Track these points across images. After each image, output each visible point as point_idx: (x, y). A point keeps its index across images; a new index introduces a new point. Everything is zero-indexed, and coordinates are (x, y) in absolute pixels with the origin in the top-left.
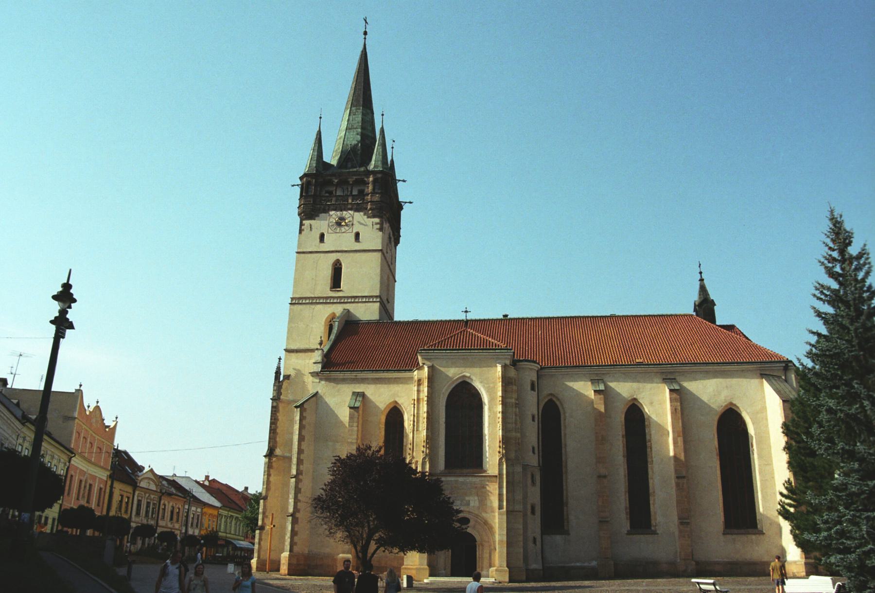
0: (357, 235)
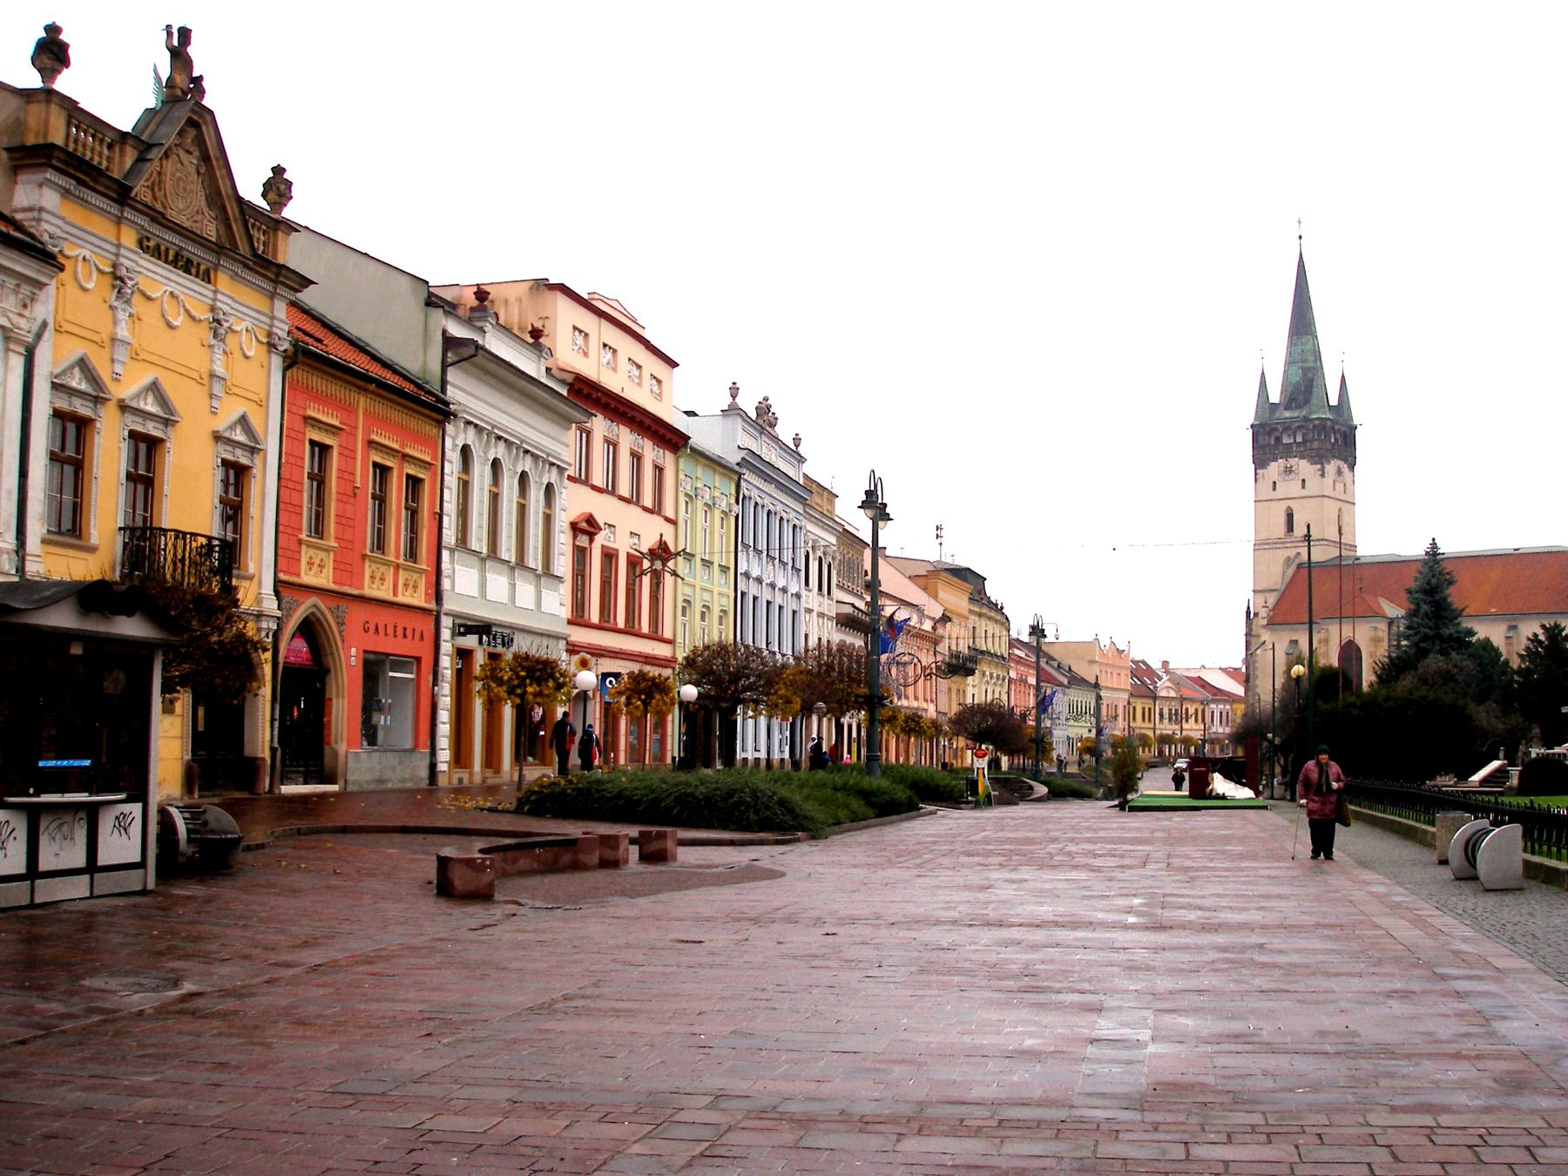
0: (1304, 480)
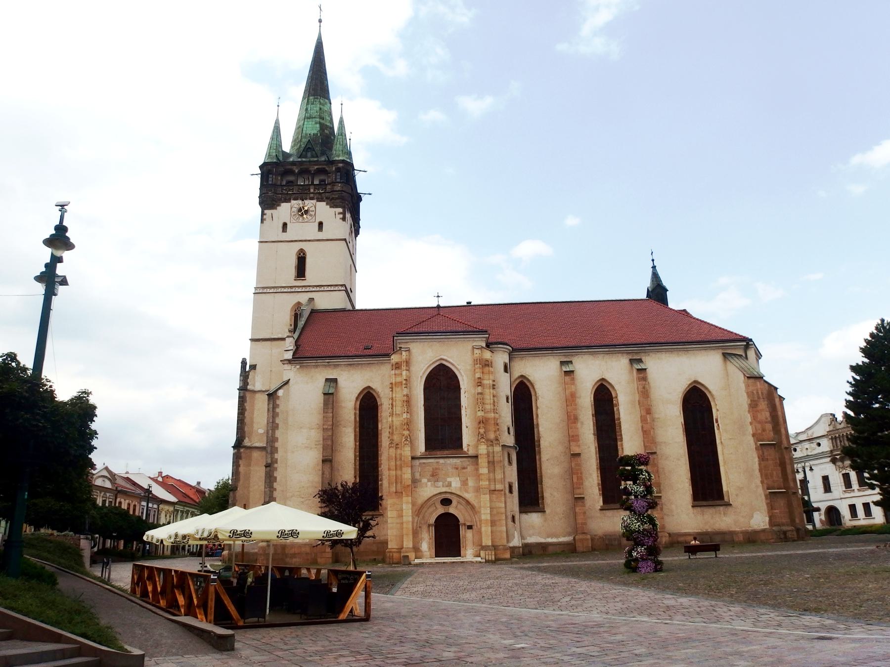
0: (321, 224)
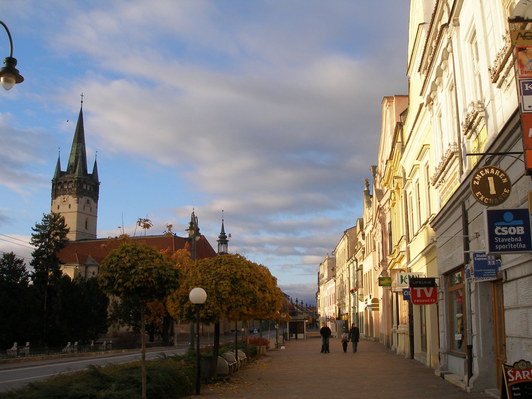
0: (70, 205)
